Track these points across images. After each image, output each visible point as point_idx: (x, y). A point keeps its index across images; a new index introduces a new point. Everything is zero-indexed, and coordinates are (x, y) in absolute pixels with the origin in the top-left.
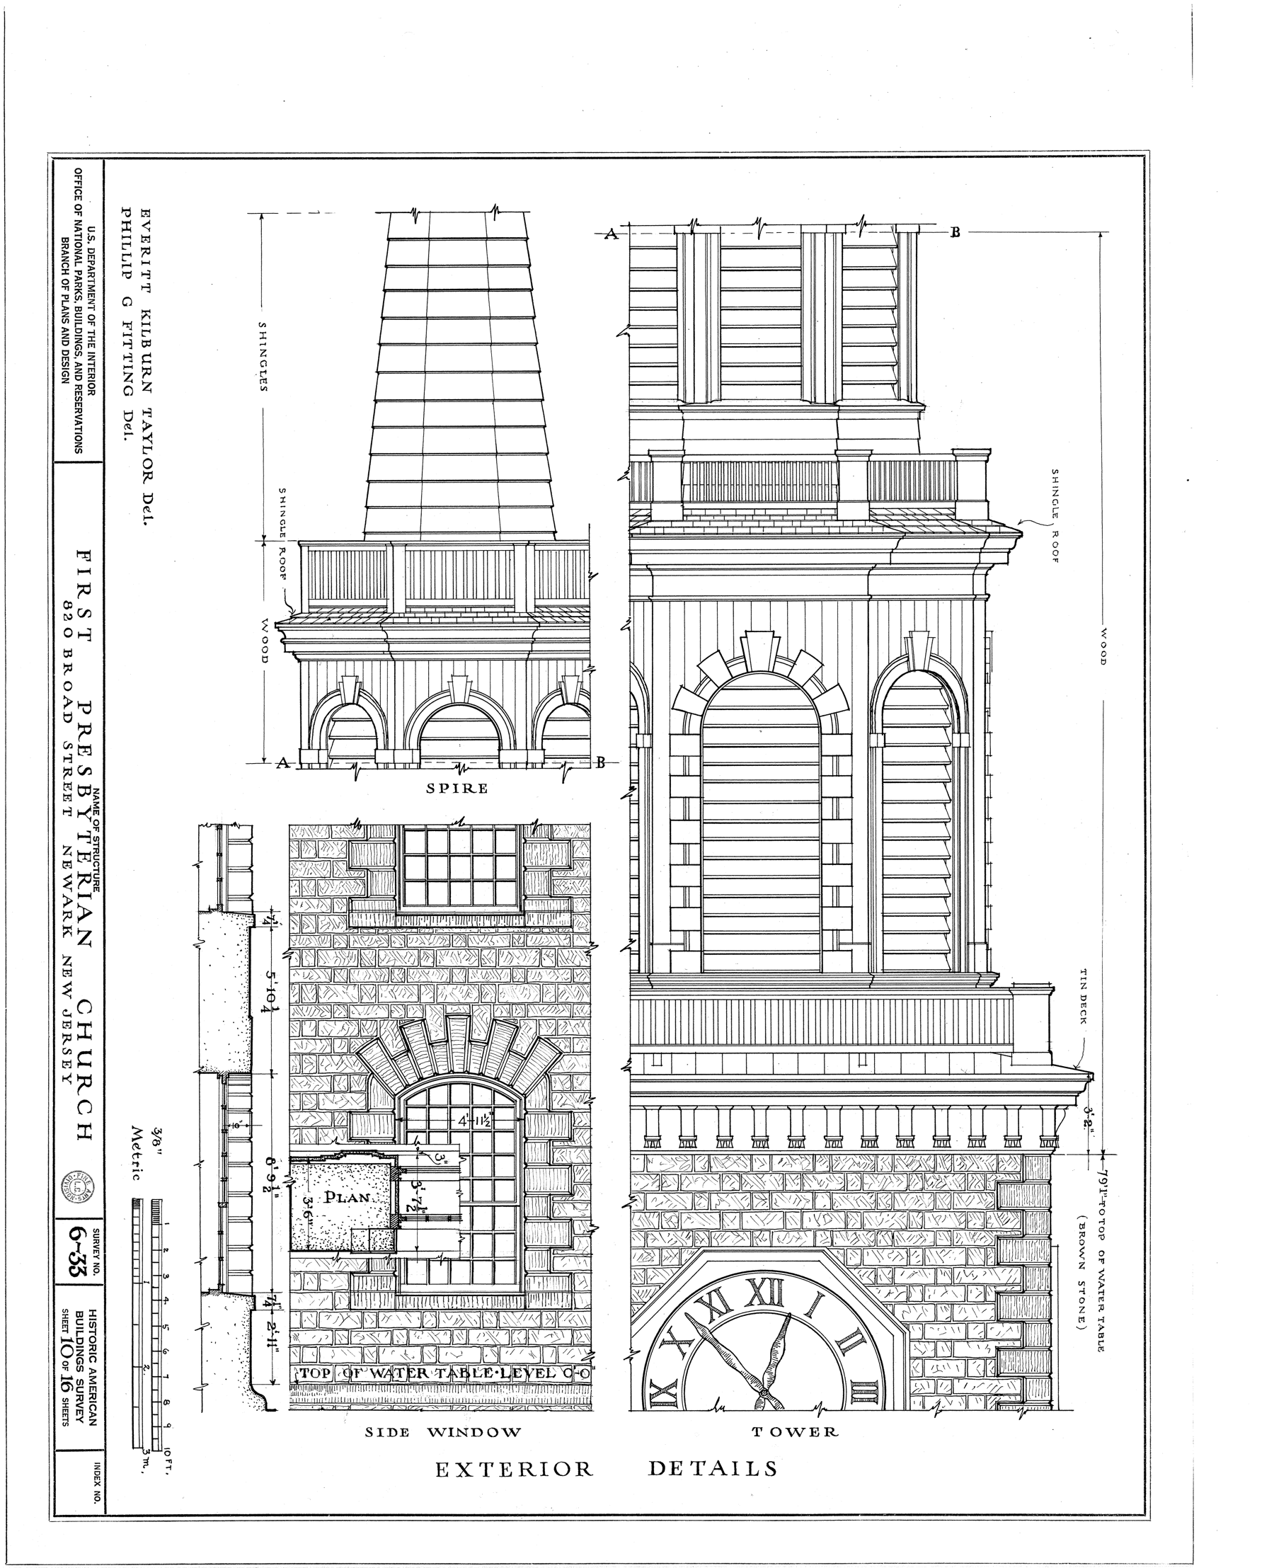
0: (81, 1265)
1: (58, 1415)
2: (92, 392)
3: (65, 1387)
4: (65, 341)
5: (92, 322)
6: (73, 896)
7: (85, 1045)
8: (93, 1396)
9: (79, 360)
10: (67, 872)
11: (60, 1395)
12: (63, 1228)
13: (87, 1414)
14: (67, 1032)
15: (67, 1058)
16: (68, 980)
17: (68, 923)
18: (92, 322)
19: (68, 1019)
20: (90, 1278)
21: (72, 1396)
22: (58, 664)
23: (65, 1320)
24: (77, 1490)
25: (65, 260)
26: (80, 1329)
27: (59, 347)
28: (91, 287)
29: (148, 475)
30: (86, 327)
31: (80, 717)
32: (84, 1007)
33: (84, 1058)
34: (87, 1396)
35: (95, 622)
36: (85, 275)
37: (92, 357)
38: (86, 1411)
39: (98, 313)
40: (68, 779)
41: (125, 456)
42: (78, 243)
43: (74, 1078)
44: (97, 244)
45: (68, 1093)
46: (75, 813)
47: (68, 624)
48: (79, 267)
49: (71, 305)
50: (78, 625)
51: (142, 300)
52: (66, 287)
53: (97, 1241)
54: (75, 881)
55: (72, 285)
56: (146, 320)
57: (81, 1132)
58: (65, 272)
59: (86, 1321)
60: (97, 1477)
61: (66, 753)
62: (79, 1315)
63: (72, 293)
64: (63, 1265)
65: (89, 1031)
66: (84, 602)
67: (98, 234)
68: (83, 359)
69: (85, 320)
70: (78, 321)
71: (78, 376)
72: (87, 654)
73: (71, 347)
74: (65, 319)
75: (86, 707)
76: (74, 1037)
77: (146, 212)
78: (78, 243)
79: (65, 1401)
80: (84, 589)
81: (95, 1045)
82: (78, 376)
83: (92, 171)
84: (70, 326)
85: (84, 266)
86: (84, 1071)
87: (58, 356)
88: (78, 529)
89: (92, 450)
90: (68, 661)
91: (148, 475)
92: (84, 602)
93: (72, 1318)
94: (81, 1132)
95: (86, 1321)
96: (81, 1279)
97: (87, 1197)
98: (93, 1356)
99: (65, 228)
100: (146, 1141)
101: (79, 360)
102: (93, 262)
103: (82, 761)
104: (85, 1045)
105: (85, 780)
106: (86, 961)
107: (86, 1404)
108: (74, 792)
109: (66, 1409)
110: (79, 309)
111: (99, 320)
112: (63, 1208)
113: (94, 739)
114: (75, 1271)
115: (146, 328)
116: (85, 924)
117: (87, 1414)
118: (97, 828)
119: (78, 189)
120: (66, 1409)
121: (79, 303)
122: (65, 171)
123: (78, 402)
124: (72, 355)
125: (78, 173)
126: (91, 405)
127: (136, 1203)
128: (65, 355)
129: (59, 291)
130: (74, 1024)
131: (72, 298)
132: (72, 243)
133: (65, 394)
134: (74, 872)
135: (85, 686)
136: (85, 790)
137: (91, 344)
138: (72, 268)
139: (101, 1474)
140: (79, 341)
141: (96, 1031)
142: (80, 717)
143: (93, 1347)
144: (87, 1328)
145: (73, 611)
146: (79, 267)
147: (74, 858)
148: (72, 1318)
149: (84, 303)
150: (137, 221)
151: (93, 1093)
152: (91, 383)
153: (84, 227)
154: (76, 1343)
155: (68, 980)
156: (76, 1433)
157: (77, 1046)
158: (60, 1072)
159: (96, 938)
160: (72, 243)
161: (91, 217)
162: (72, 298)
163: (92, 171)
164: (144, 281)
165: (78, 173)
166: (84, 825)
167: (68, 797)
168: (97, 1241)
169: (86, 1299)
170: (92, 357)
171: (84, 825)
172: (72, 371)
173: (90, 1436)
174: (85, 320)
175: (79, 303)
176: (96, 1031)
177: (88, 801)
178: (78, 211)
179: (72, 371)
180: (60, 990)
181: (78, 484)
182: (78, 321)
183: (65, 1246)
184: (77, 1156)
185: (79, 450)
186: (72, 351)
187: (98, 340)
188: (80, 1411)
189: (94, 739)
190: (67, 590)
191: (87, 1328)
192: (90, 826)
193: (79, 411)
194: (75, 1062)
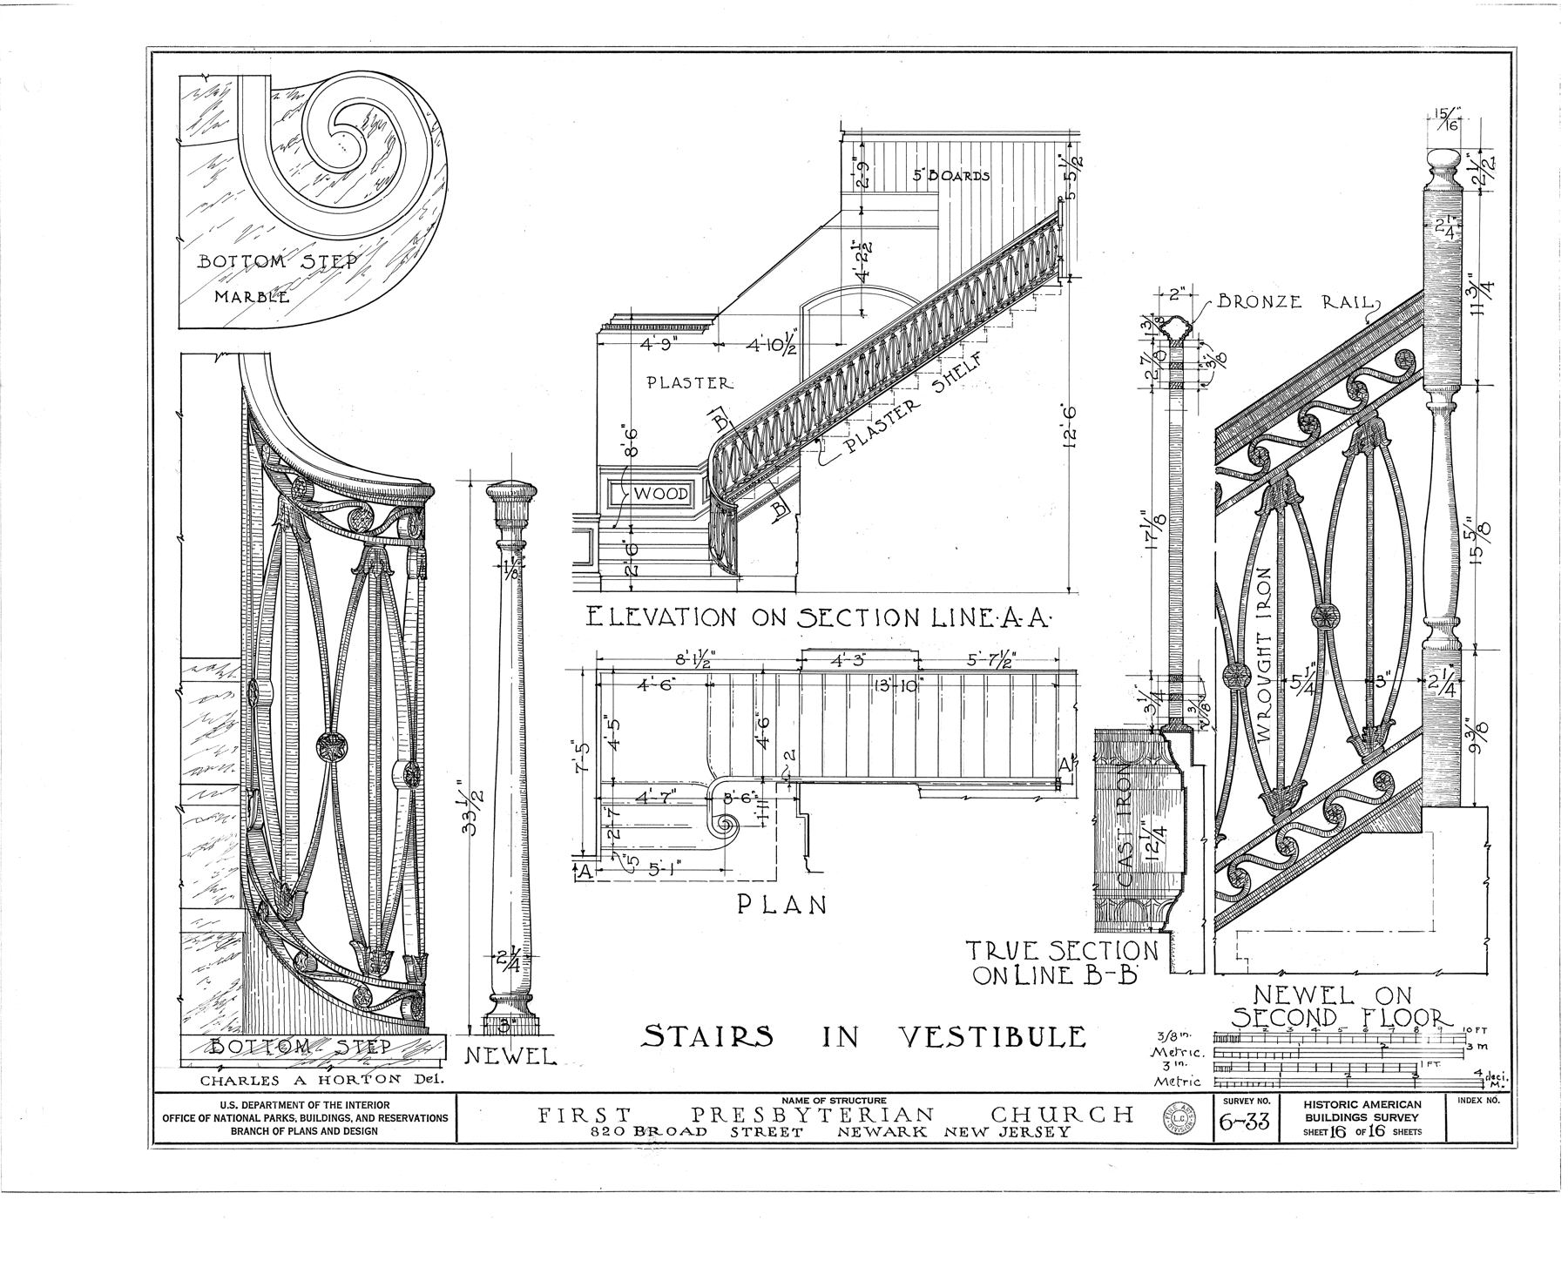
0: (1259, 1119)
1: (1409, 1140)
2: (387, 1105)
4: (334, 1131)
5: (316, 1105)
6: (885, 1127)
7: (1034, 1114)
8: (1391, 1104)
9: (353, 1117)
10: (863, 1132)
11: (1389, 1137)
13: (1410, 1111)
14: (1019, 1132)
16: (970, 1132)
17: (910, 1131)
18: (316, 1105)
21: (1390, 1126)
23: (1315, 1132)
25: (254, 1131)
26: (1324, 1118)
27: (341, 1138)
28: (282, 1105)
30: (321, 1110)
31: (705, 1121)
32: (999, 1115)
33: (1048, 1114)
34: (1391, 1111)
35: (611, 1103)
36: (269, 1112)
37: (351, 1105)
38: (1406, 1111)
40: (766, 1132)
42: (236, 1118)
47: (611, 1132)
48: (261, 1117)
49: (298, 1125)
50: (613, 1120)
52: (281, 1130)
53: (1236, 1101)
54: (868, 1123)
55: (279, 1124)
58: (266, 1131)
59: (1315, 1111)
60: (1473, 1101)
62: (1309, 1118)
63: (287, 1125)
65: (1021, 1110)
66: (590, 1114)
68: (353, 1113)
69: (314, 1111)
70: (315, 1118)
71: (369, 1118)
72: (645, 1112)
73: (341, 1125)
74: (313, 1131)
75: (698, 1111)
76: (1026, 1125)
78: (236, 1118)
79: (1396, 1132)
80: (578, 1114)
81: (1034, 1102)
82: (369, 1118)
83: (165, 1105)
84: (320, 1126)
85: (260, 1113)
87: (350, 1138)
88: (518, 1119)
89: (444, 1105)
92: (590, 1114)
93: (1313, 1125)
95: (1315, 1111)
98: (1351, 1105)
99: (222, 1131)
101: (353, 1117)
102: (256, 1104)
103: (749, 1117)
105: (769, 1115)
107: (1400, 1111)
108: (778, 1125)
109: (1404, 1132)
110: (303, 1118)
111: (314, 1098)
112: (1202, 1132)
116: (912, 1114)
117: (1410, 1111)
119: (183, 1118)
120: (1404, 1132)
122: (165, 1132)
123: (397, 1118)
124: (349, 1125)
125: (168, 1118)
126: (398, 1105)
128: (348, 1131)
129: (285, 1137)
131: (292, 1125)
132: (237, 1125)
133: (387, 1131)
136: (779, 1114)
137: (338, 1105)
138: (263, 1124)
140: (335, 1118)
141: (1021, 1102)
142: (705, 1121)
143: (1342, 1104)
144: (1323, 1111)
145: (600, 1126)
146: (261, 1117)
148: (1313, 1125)
149: (297, 1113)
151: (1083, 1104)
152: (376, 1105)
153: (221, 1112)
156: (1429, 1120)
160: (237, 1125)
162: (292, 1125)
163: (165, 1105)
165: (168, 1118)
166: (814, 1114)
168: (1236, 1101)
170: (351, 1105)
171: (814, 1114)
172: (365, 1125)
174: (314, 1111)
177: (790, 1109)
179: (365, 1125)
180: (980, 1138)
181: (478, 1119)
182: (315, 1118)
183: (1239, 1133)
185: (442, 1118)
186: (345, 1124)
187: (333, 1098)
190: (582, 1132)
191: (1323, 1111)
193: (405, 1117)
194: (1052, 1123)
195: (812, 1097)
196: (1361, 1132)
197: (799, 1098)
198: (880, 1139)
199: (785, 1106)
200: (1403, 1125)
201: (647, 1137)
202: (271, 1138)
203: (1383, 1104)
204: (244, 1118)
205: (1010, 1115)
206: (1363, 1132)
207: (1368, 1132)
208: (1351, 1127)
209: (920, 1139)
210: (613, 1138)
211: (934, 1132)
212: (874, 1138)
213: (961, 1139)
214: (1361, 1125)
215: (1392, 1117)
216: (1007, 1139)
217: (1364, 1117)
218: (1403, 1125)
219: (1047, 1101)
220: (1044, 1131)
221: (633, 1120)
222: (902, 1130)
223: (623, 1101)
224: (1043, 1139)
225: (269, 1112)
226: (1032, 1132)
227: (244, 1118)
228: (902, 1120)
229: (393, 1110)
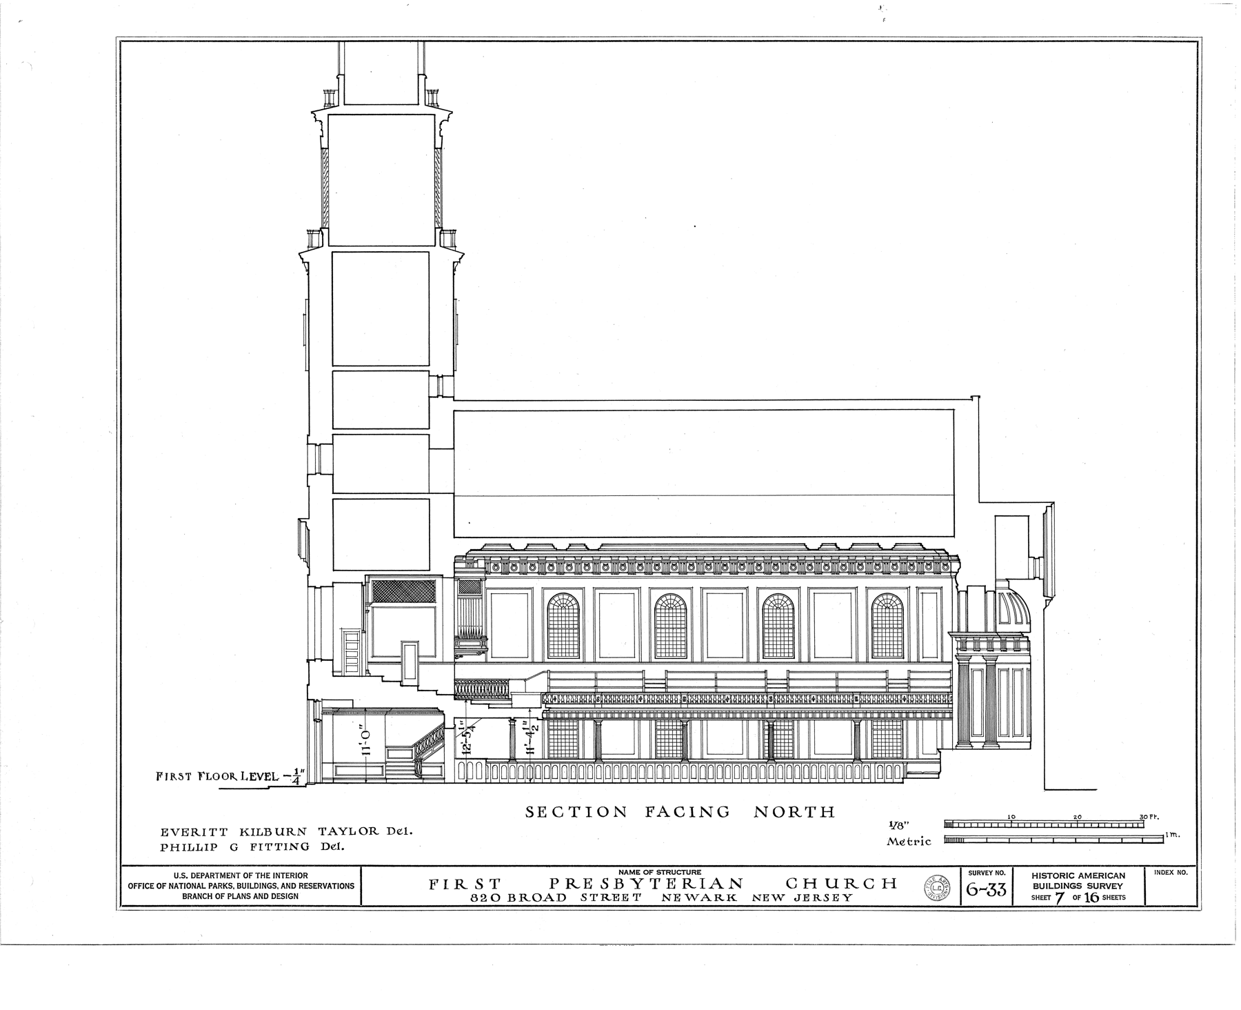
0: (997, 888)
1: (1117, 904)
2: (305, 875)
3: (1095, 899)
4: (265, 896)
5: (250, 875)
6: (702, 893)
7: (821, 883)
8: (1101, 875)
9: (279, 885)
10: (683, 898)
12: (967, 900)
14: (811, 898)
15: (831, 897)
16: (771, 897)
17: (725, 897)
18: (250, 875)
19: (802, 897)
20: (1006, 879)
21: (1101, 892)
22: (519, 902)
23: (1040, 898)
24: (1178, 889)
25: (201, 896)
26: (1048, 886)
27: (269, 901)
28: (223, 876)
29: (372, 831)
31: (561, 887)
32: (792, 883)
33: (832, 884)
34: (1101, 881)
36: (213, 881)
37: (277, 875)
38: (1113, 881)
39: (242, 870)
41: (356, 849)
42: (186, 886)
43: (847, 892)
44: (188, 871)
45: (859, 896)
46: (637, 891)
47: (488, 898)
49: (236, 892)
51: (233, 836)
52: (222, 896)
53: (978, 873)
54: (689, 891)
55: (220, 891)
56: (250, 832)
57: (889, 886)
58: (210, 896)
59: (1041, 881)
60: (1166, 873)
61: (590, 899)
62: (1036, 886)
63: (226, 891)
64: (996, 901)
66: (470, 883)
67: (180, 870)
68: (279, 882)
71: (292, 886)
72: (512, 883)
73: (269, 891)
74: (247, 896)
75: (553, 882)
76: (816, 892)
77: (164, 832)
78: (186, 886)
79: (1105, 897)
80: (459, 884)
81: (820, 875)
82: (292, 886)
83: (130, 875)
84: (252, 892)
85: (206, 881)
86: (842, 884)
88: (413, 887)
89: (352, 875)
90: (518, 897)
91: (372, 831)
92: (470, 883)
93: (1039, 892)
94: (889, 886)
95: (1041, 881)
96: (1008, 887)
97: (945, 881)
98: (1069, 876)
99: (175, 896)
100: (898, 834)
101: (279, 885)
102: (202, 874)
103: (596, 889)
104: (821, 883)
105: (612, 883)
106: (755, 883)
107: (1108, 881)
109: (1112, 897)
110: (239, 886)
111: (248, 870)
112: (953, 899)
113: (579, 875)
114: (1002, 892)
115: (256, 832)
116: (726, 883)
118: (650, 872)
119: (145, 886)
120: (1112, 897)
121: (235, 885)
122: (130, 897)
123: (314, 886)
124: (276, 891)
125: (132, 886)
126: (315, 876)
127: (948, 840)
128: (275, 896)
129: (225, 901)
130: (806, 892)
131: (231, 891)
132: (187, 891)
133: (306, 896)
134: (683, 892)
135: (536, 883)
136: (619, 883)
137: (267, 875)
138: (207, 891)
139: (1164, 870)
140: (265, 886)
141: (810, 874)
142: (561, 887)
143: (1062, 875)
144: (1047, 881)
147: (672, 891)
148: (1039, 892)
149: (234, 881)
150: (171, 839)
151: (859, 875)
152: (297, 876)
153: (175, 881)
154: (1055, 886)
155: (771, 897)
156: (1131, 889)
157: (822, 890)
158: (842, 901)
159: (736, 873)
160: (187, 891)
161: (167, 876)
162: (231, 891)
163: (130, 875)
164: (218, 833)
165: (132, 886)
166: (646, 885)
167: (625, 897)
168: (978, 873)
169: (1024, 879)
170: (277, 875)
171: (646, 885)
172: (288, 891)
173: (1134, 875)
175: (235, 885)
176: (810, 874)
177: (626, 879)
178: (162, 886)
179: (288, 891)
180: (778, 902)
181: (378, 887)
183: (982, 899)
184: (912, 887)
185: (351, 886)
186: (273, 891)
187: (263, 870)
188: (1113, 886)
189: (579, 875)
190: (463, 897)
191: (1047, 881)
192: (649, 877)
193: (320, 885)
194: (835, 891)
195: (642, 869)
196: (1078, 897)
197: (634, 870)
198: (698, 902)
199: (621, 876)
200: (1111, 892)
201: (519, 902)
202: (214, 901)
203: (1094, 876)
204: (193, 886)
205: (801, 883)
206: (1078, 897)
207: (1084, 898)
208: (1069, 893)
209: (732, 903)
210: (489, 902)
211: (743, 897)
212: (692, 902)
213: (762, 902)
214: (1076, 892)
215: (1102, 886)
216: (801, 902)
217: (1079, 886)
218: (1111, 892)
219: (832, 874)
220: (831, 897)
221: (503, 890)
222: (718, 897)
223: (494, 873)
224: (830, 903)
225: (213, 881)
226: (822, 897)
227: (193, 886)
228: (716, 890)
229: (310, 880)
